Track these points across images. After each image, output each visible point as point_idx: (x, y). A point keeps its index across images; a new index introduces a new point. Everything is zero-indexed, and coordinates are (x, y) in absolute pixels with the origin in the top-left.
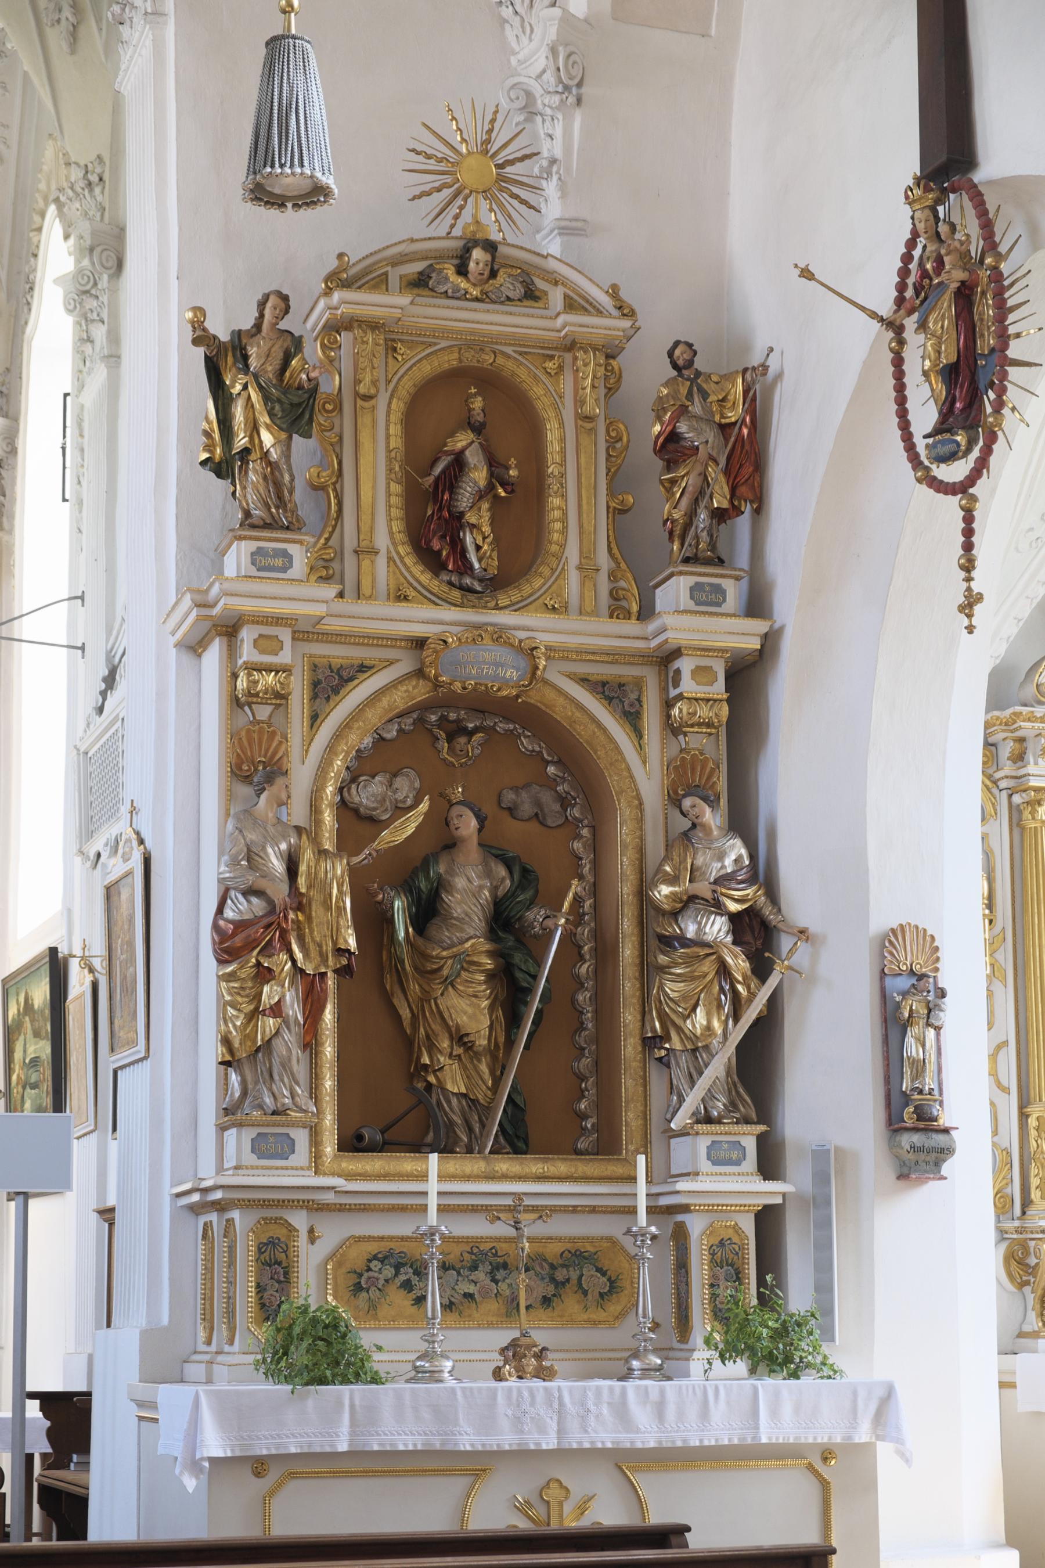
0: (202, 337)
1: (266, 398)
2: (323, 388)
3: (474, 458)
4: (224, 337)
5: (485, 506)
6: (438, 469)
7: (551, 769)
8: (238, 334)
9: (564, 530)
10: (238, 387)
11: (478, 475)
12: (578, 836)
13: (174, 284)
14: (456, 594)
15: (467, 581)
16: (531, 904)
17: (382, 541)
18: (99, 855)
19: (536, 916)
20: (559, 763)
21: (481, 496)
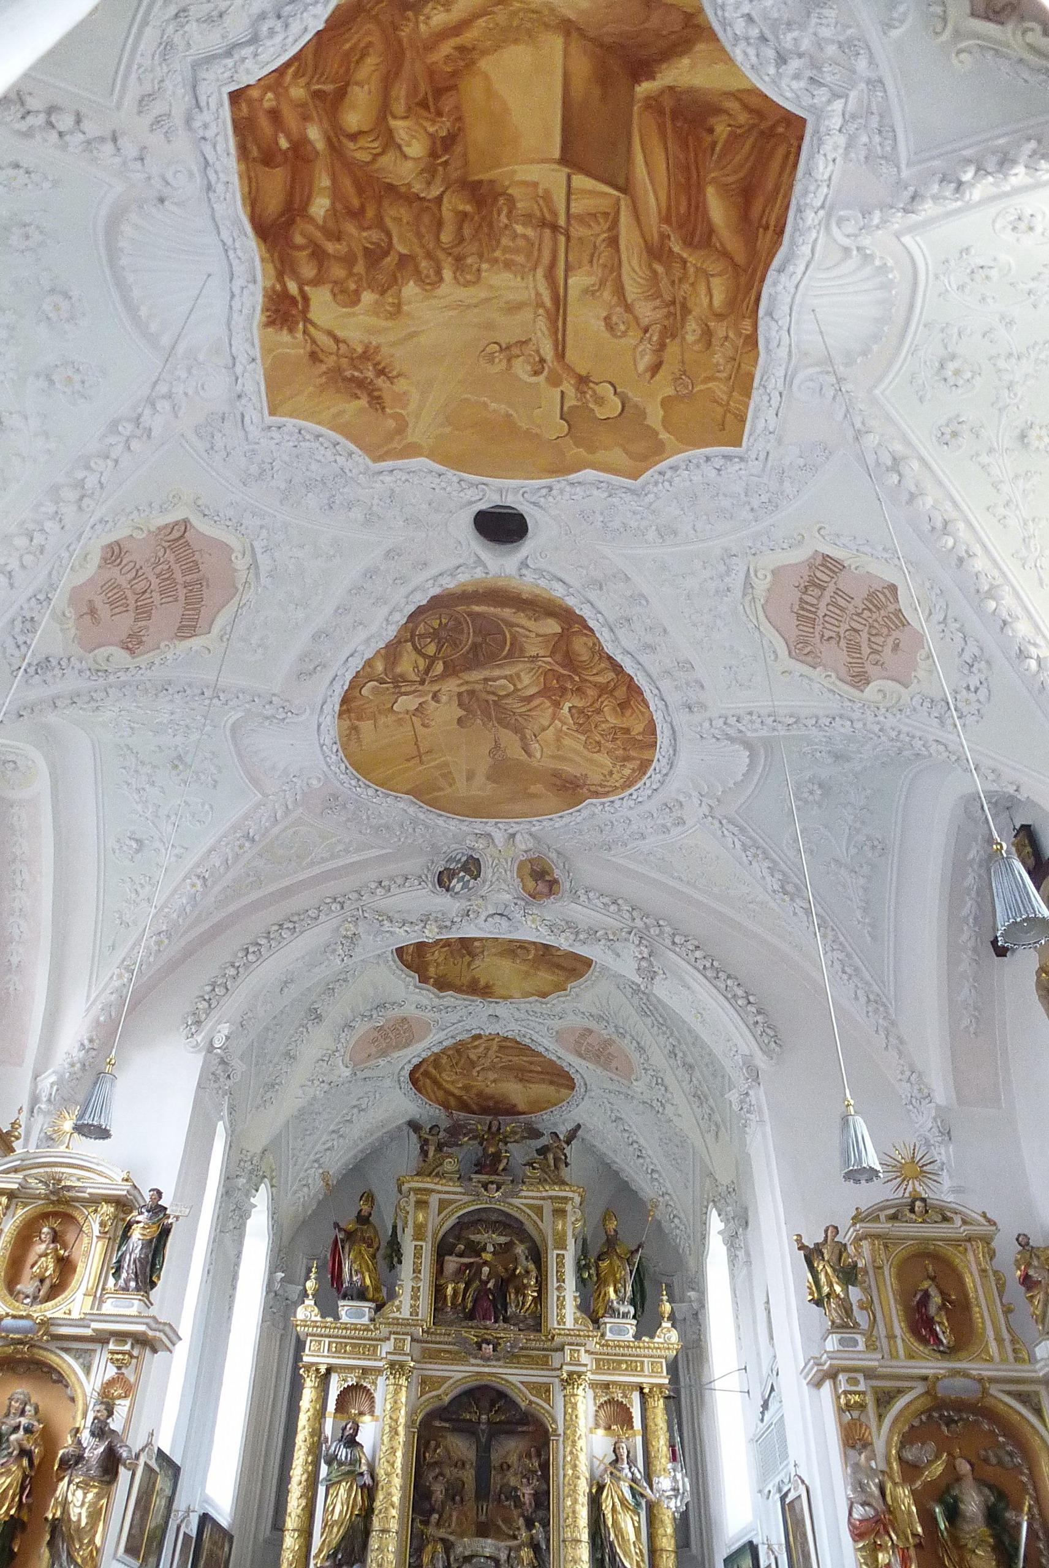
0: (802, 1247)
1: (834, 1270)
2: (860, 1265)
3: (933, 1291)
4: (812, 1246)
5: (943, 1313)
6: (918, 1297)
7: (1001, 1439)
8: (817, 1244)
9: (983, 1323)
10: (821, 1267)
11: (937, 1300)
12: (1022, 1474)
13: (783, 1226)
14: (938, 1355)
15: (942, 1348)
16: (1006, 1508)
17: (898, 1332)
18: (770, 1492)
19: (1010, 1515)
20: (1004, 1436)
21: (940, 1309)
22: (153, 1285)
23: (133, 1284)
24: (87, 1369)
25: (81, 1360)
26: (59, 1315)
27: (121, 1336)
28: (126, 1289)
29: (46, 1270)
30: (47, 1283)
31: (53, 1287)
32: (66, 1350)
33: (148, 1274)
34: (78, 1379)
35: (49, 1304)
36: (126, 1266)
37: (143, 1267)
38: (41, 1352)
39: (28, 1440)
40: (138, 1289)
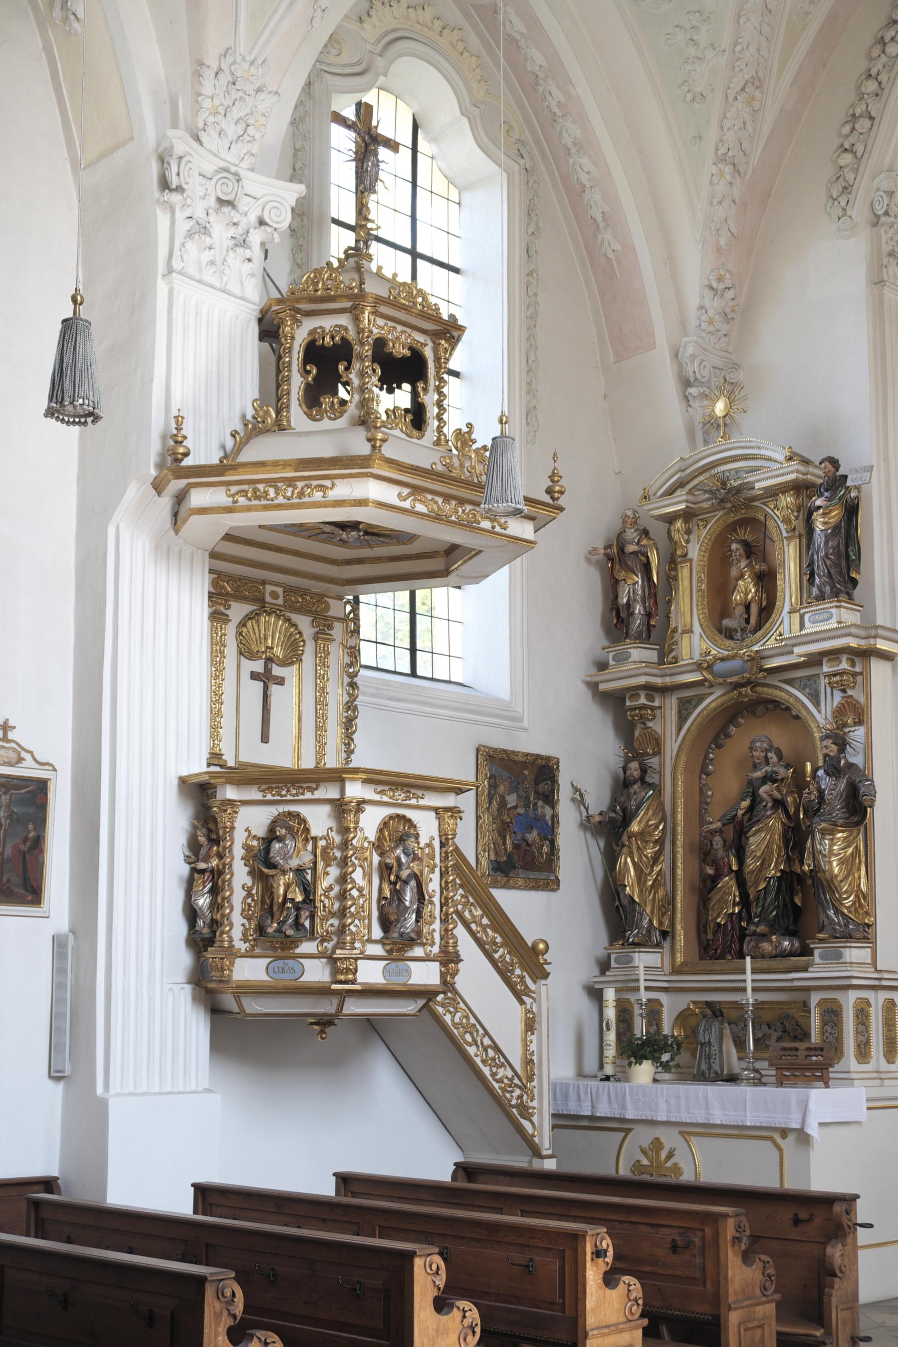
22: (854, 582)
23: (828, 589)
24: (815, 698)
25: (807, 690)
26: (771, 644)
27: (834, 654)
28: (821, 598)
29: (746, 594)
30: (754, 610)
31: (761, 610)
32: (789, 682)
33: (844, 570)
34: (810, 712)
35: (760, 633)
36: (816, 569)
37: (836, 565)
38: (765, 689)
39: (778, 789)
40: (836, 594)
